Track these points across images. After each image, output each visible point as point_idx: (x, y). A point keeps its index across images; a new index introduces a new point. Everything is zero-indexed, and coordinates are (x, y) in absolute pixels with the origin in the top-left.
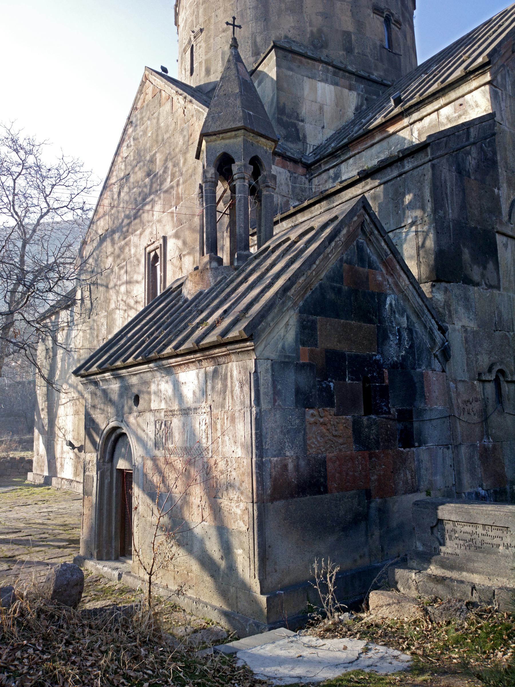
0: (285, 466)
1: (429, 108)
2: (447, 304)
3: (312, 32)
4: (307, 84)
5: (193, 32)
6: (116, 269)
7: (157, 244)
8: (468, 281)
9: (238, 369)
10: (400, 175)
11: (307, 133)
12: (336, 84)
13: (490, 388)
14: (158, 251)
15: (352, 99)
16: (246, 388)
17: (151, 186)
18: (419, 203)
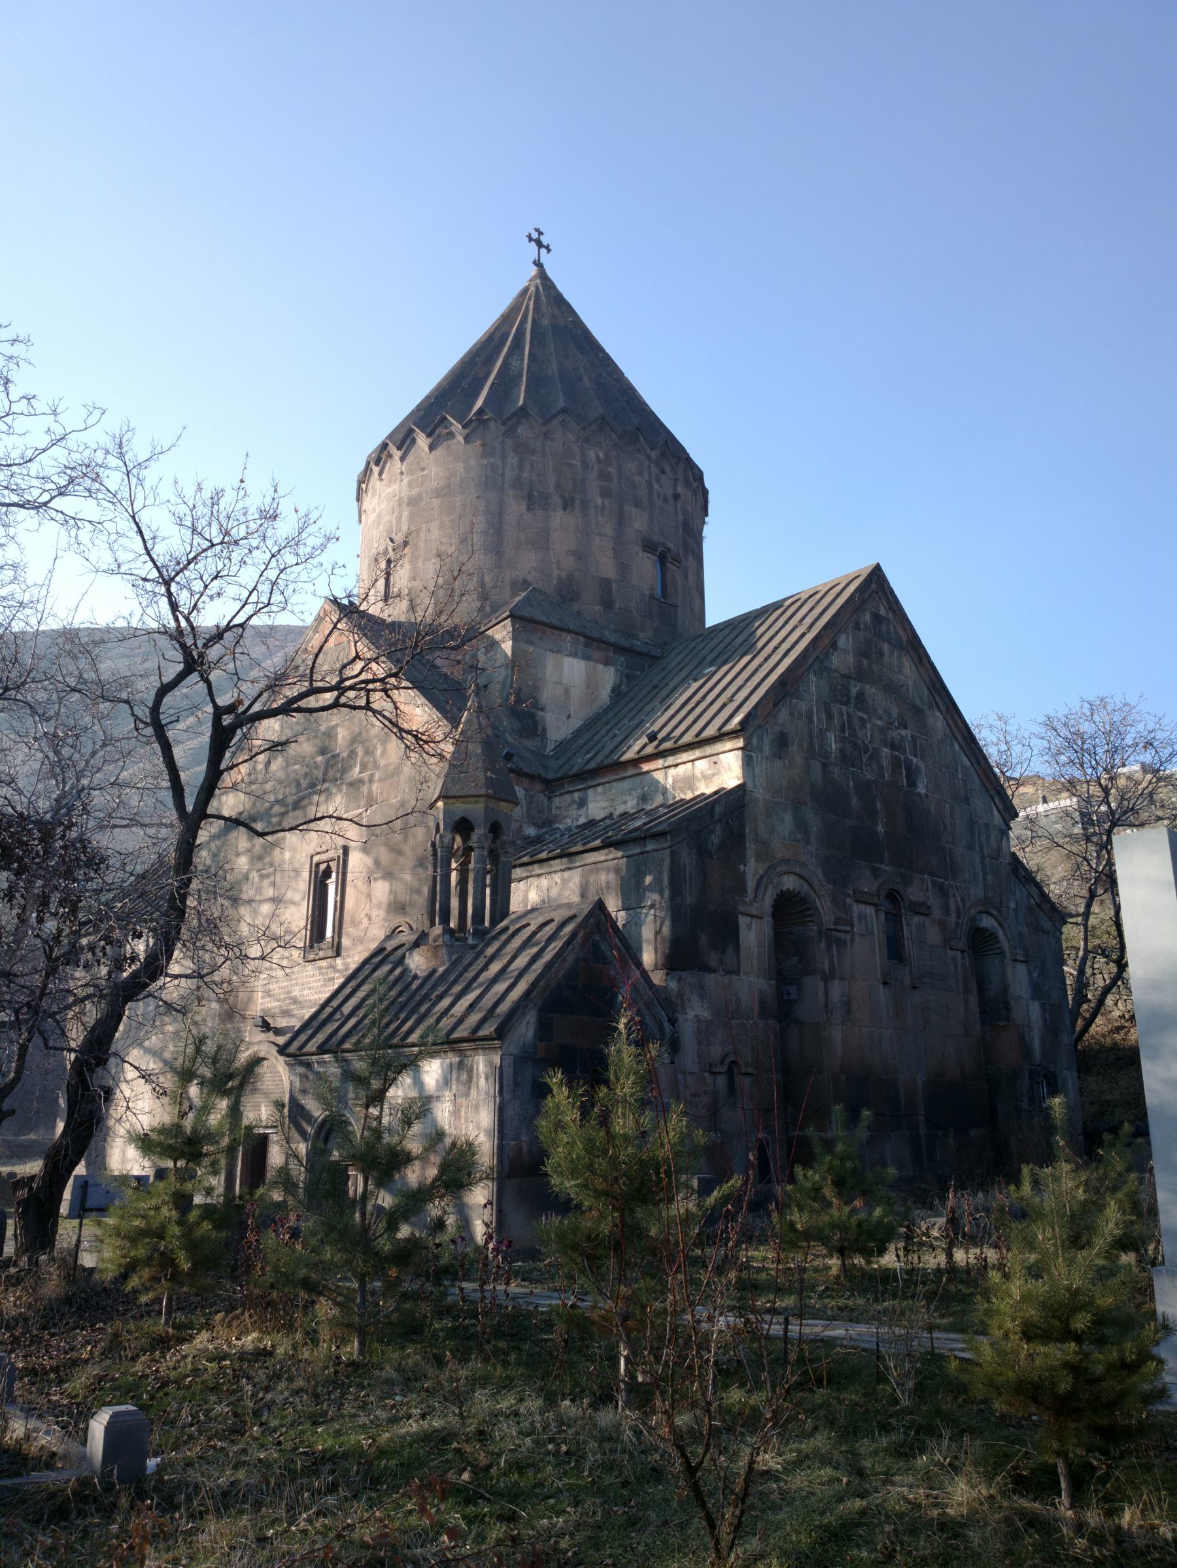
0: (521, 1149)
1: (685, 756)
2: (680, 994)
3: (559, 577)
4: (550, 660)
5: (392, 540)
6: (254, 876)
7: (331, 854)
8: (706, 968)
9: (482, 1063)
10: (642, 853)
11: (548, 725)
12: (587, 658)
13: (722, 1081)
14: (333, 865)
15: (608, 677)
16: (491, 1080)
17: (326, 770)
18: (657, 887)
